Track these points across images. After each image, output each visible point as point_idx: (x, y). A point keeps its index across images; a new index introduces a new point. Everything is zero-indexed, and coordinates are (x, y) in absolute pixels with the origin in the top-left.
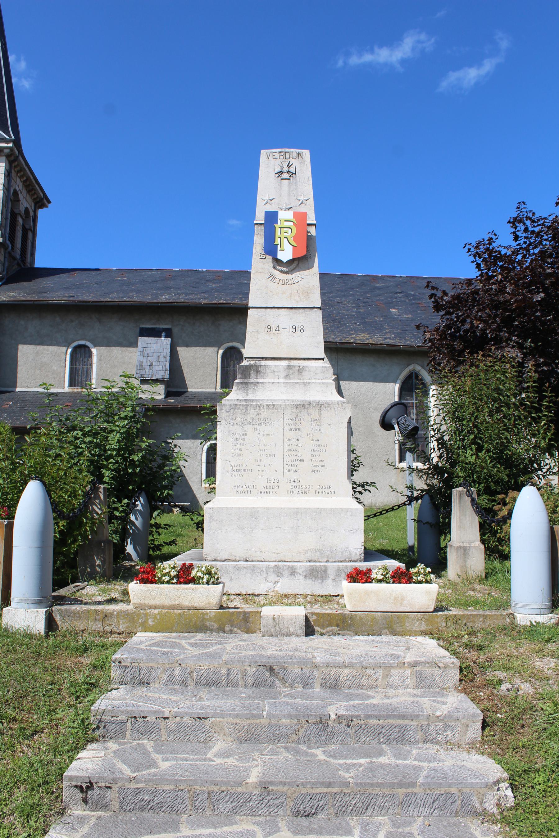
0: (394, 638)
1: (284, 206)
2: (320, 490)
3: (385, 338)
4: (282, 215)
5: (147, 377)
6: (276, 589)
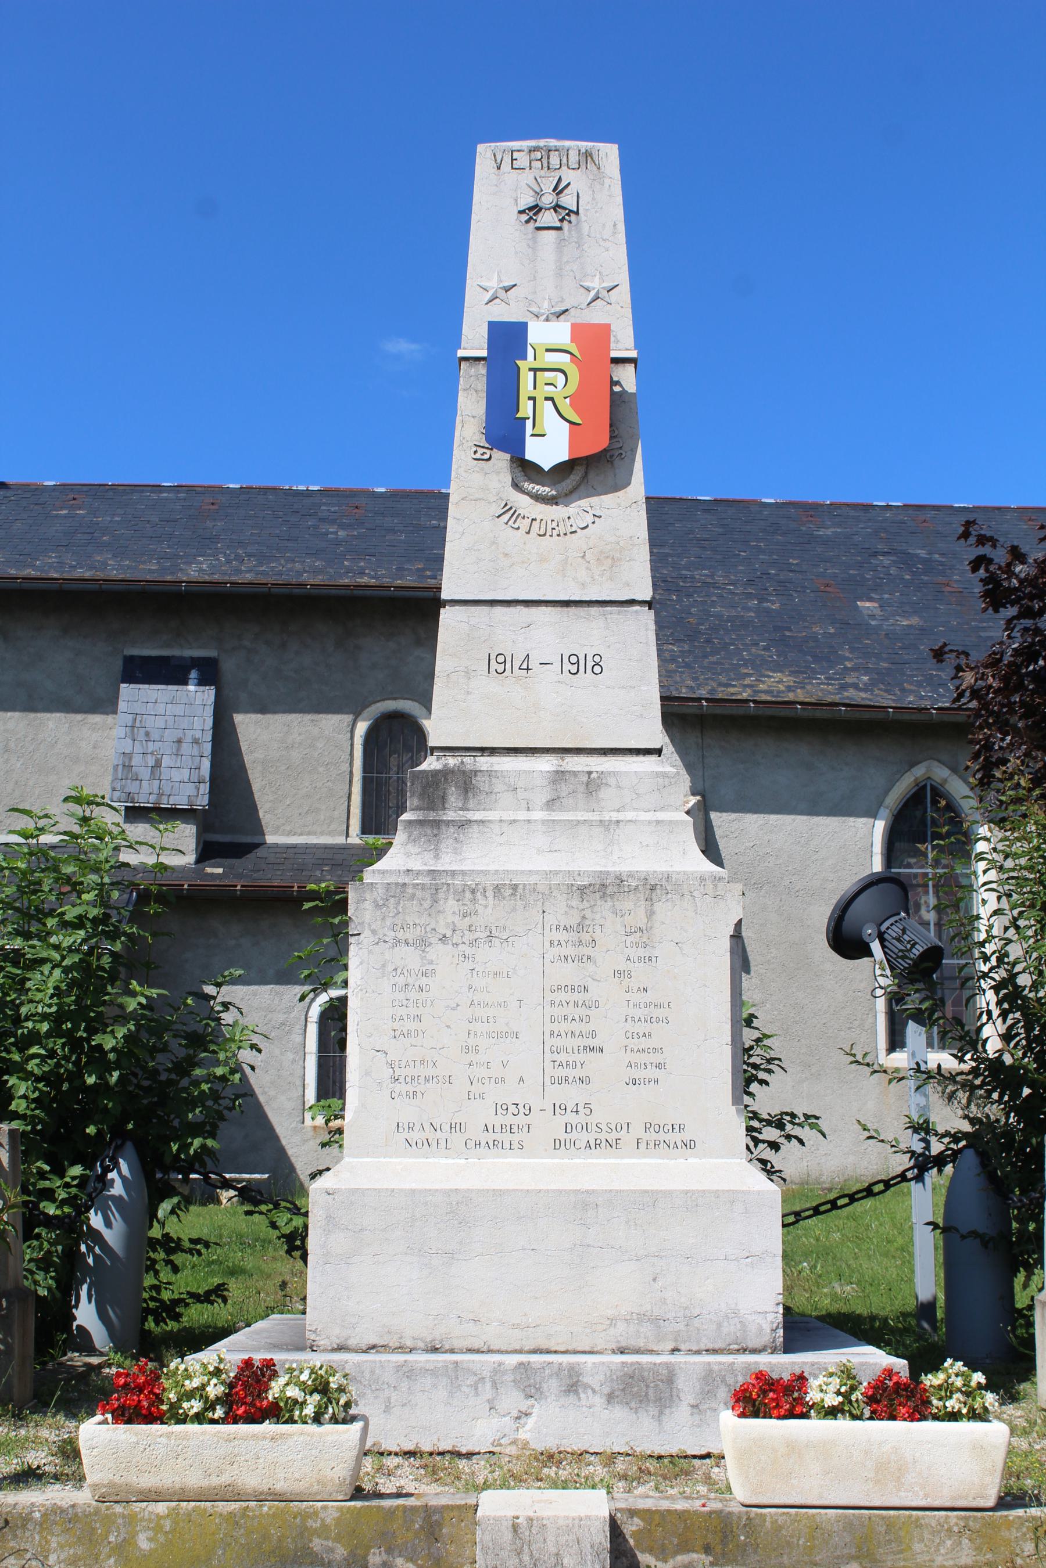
1: (545, 307)
2: (652, 1136)
3: (844, 687)
4: (539, 334)
5: (145, 799)
6: (522, 1435)
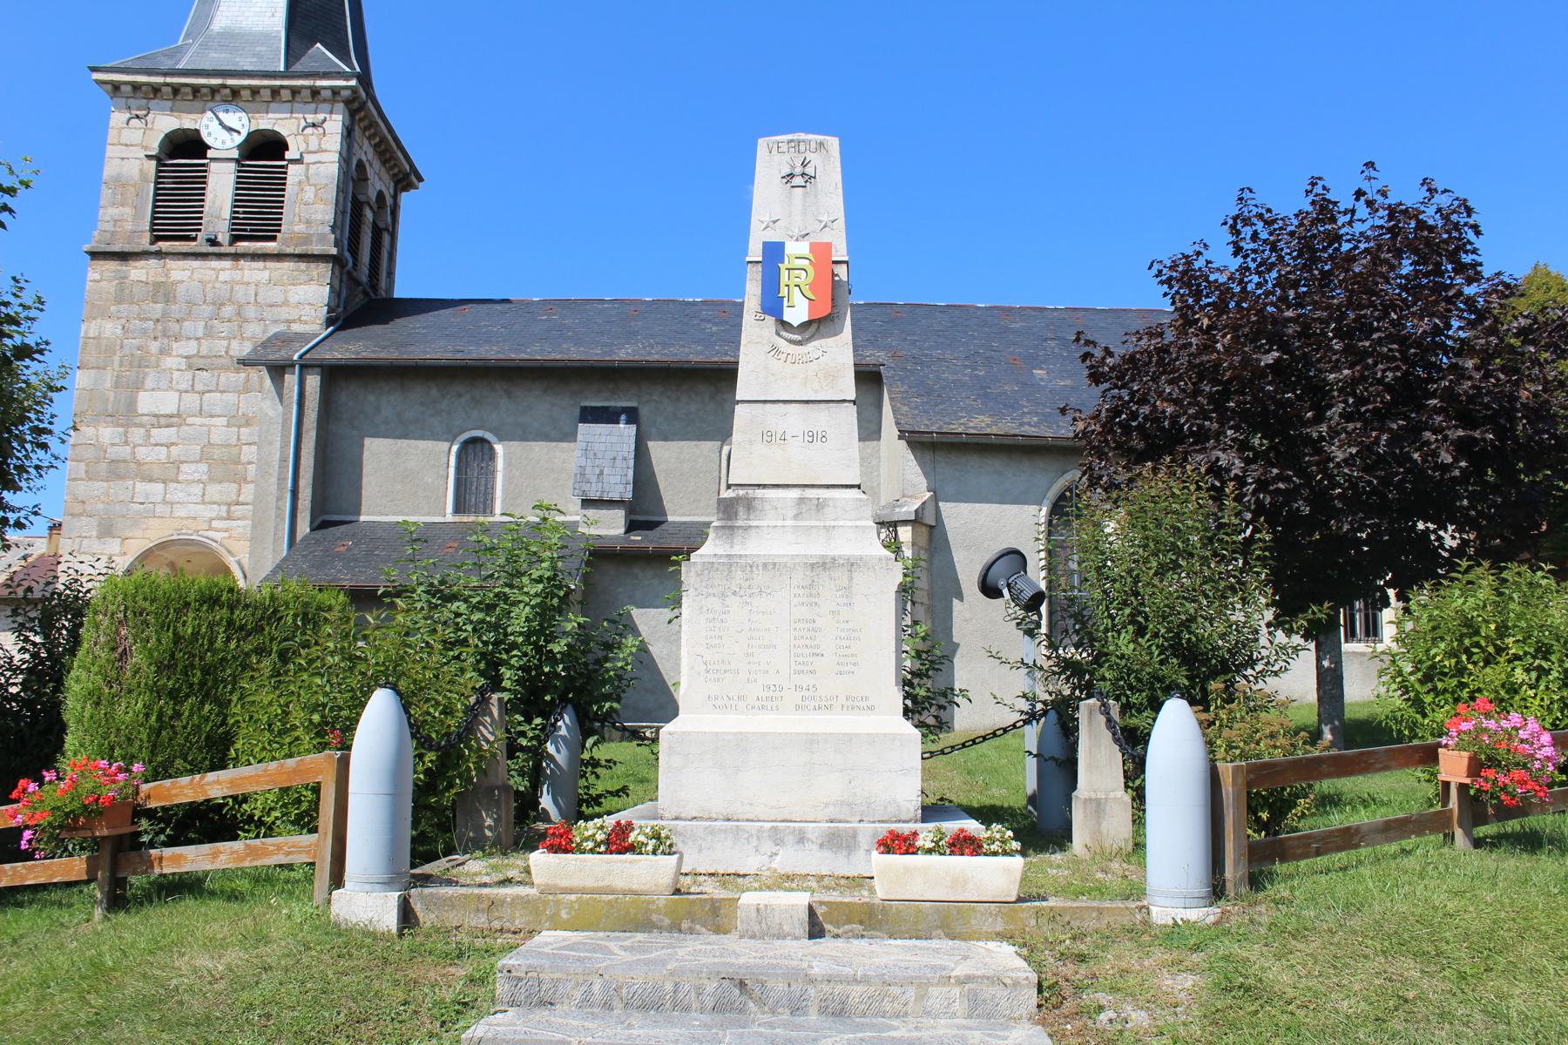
0: (950, 943)
1: (796, 232)
2: (850, 703)
3: (1022, 425)
4: (792, 248)
5: (594, 495)
6: (773, 865)
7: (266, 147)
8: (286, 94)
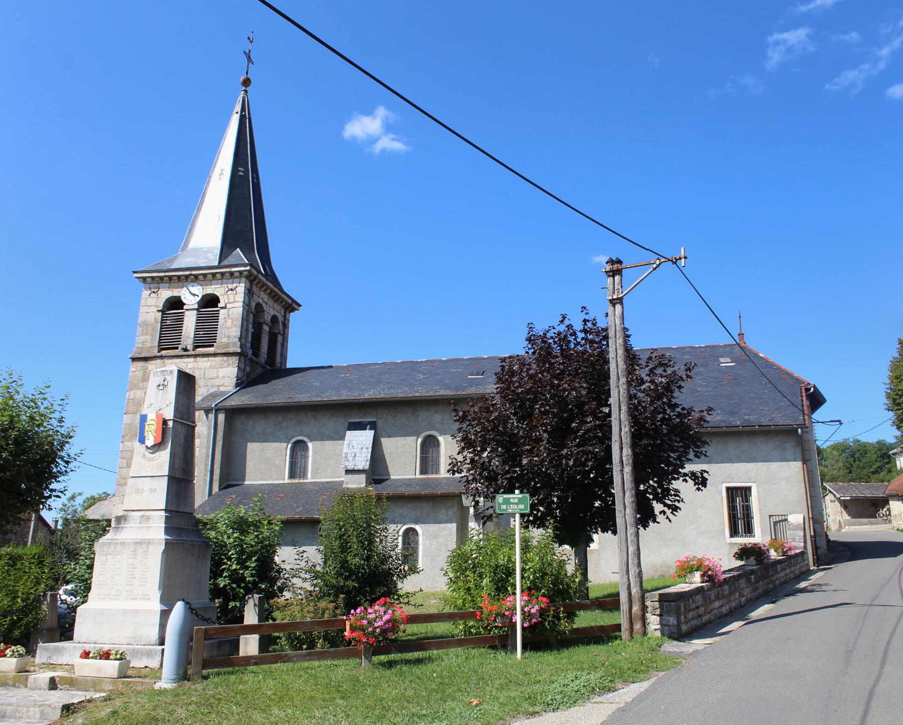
4: (149, 417)
5: (350, 467)
7: (210, 301)
8: (219, 276)
